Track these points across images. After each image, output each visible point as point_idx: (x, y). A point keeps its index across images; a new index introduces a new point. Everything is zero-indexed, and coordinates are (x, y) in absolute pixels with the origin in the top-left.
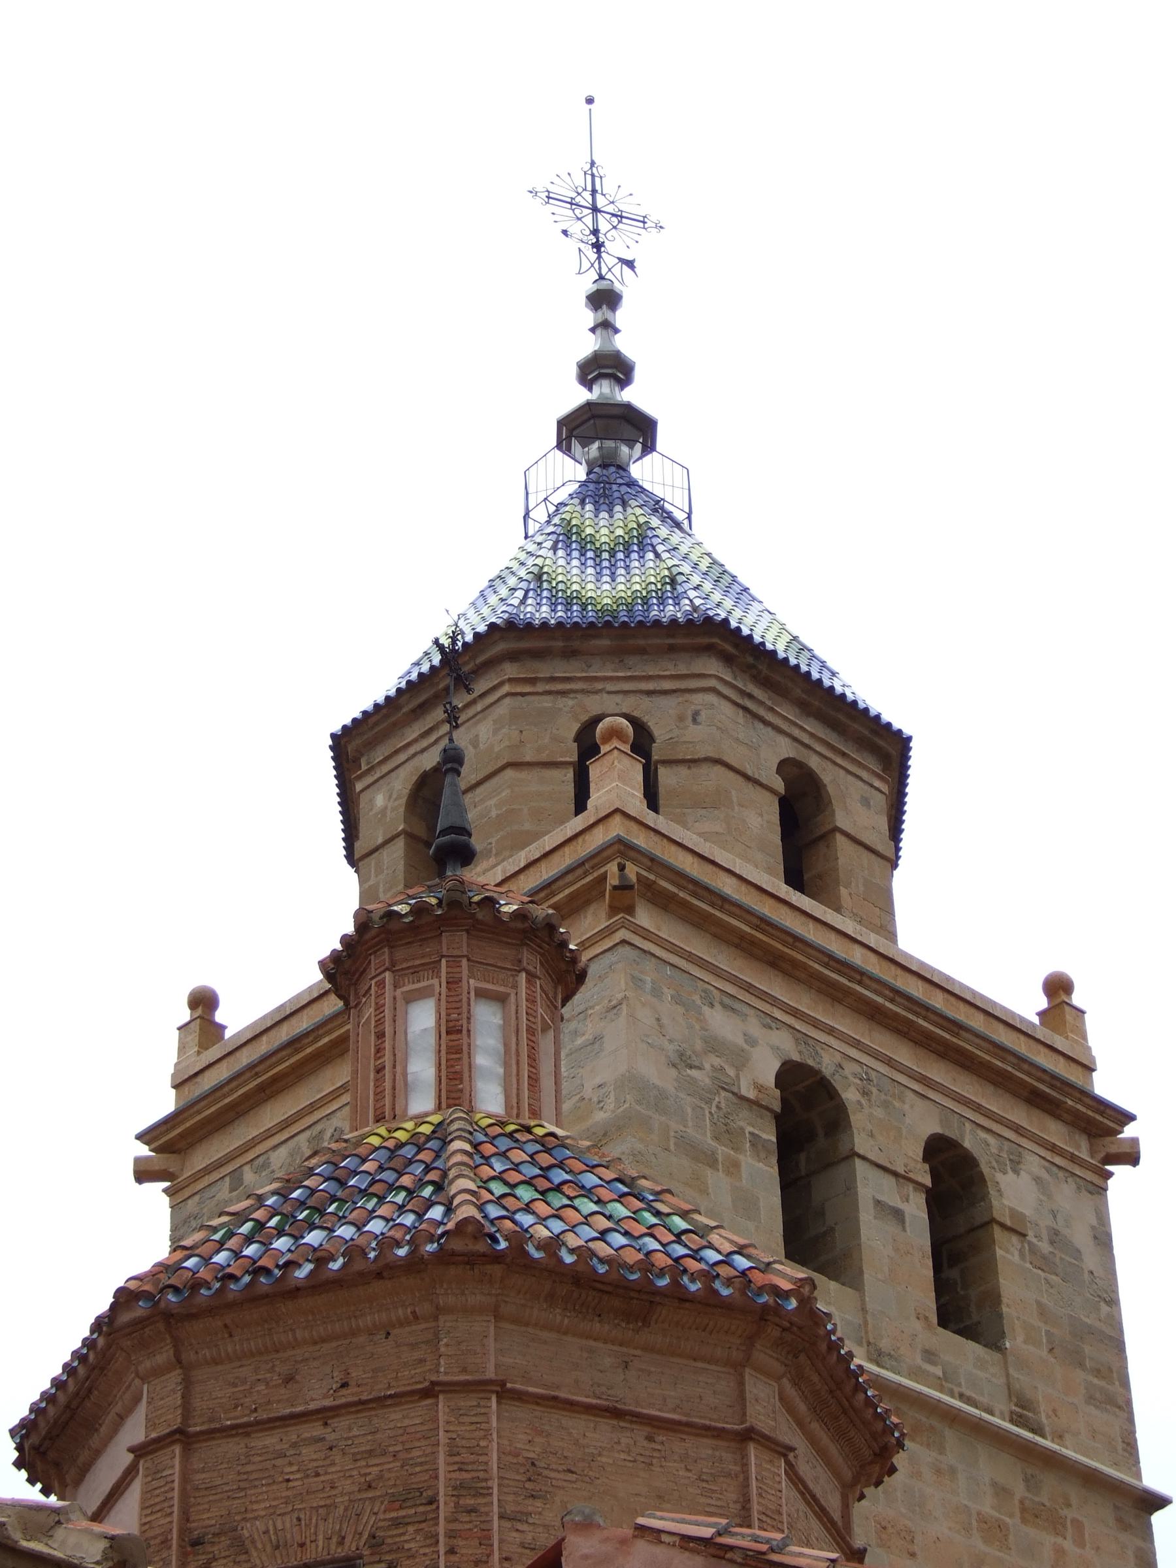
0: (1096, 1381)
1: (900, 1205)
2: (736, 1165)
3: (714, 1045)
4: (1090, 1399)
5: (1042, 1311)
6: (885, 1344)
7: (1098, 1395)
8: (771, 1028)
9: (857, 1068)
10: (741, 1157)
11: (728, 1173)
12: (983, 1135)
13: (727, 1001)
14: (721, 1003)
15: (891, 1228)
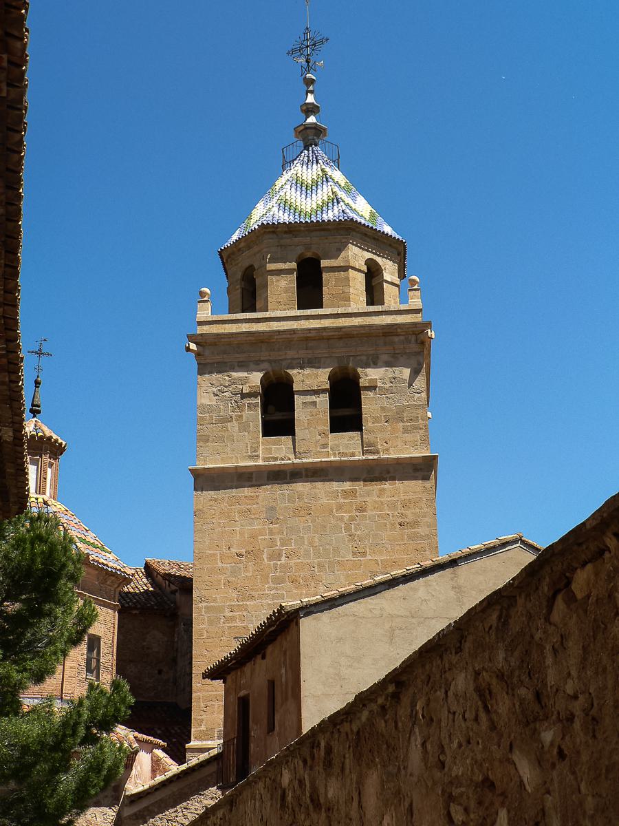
0: (409, 424)
1: (316, 400)
2: (241, 416)
3: (233, 382)
4: (405, 431)
5: (383, 409)
6: (301, 451)
7: (409, 429)
8: (259, 364)
9: (299, 361)
10: (243, 413)
11: (237, 420)
12: (358, 358)
13: (240, 364)
14: (238, 366)
15: (310, 409)
